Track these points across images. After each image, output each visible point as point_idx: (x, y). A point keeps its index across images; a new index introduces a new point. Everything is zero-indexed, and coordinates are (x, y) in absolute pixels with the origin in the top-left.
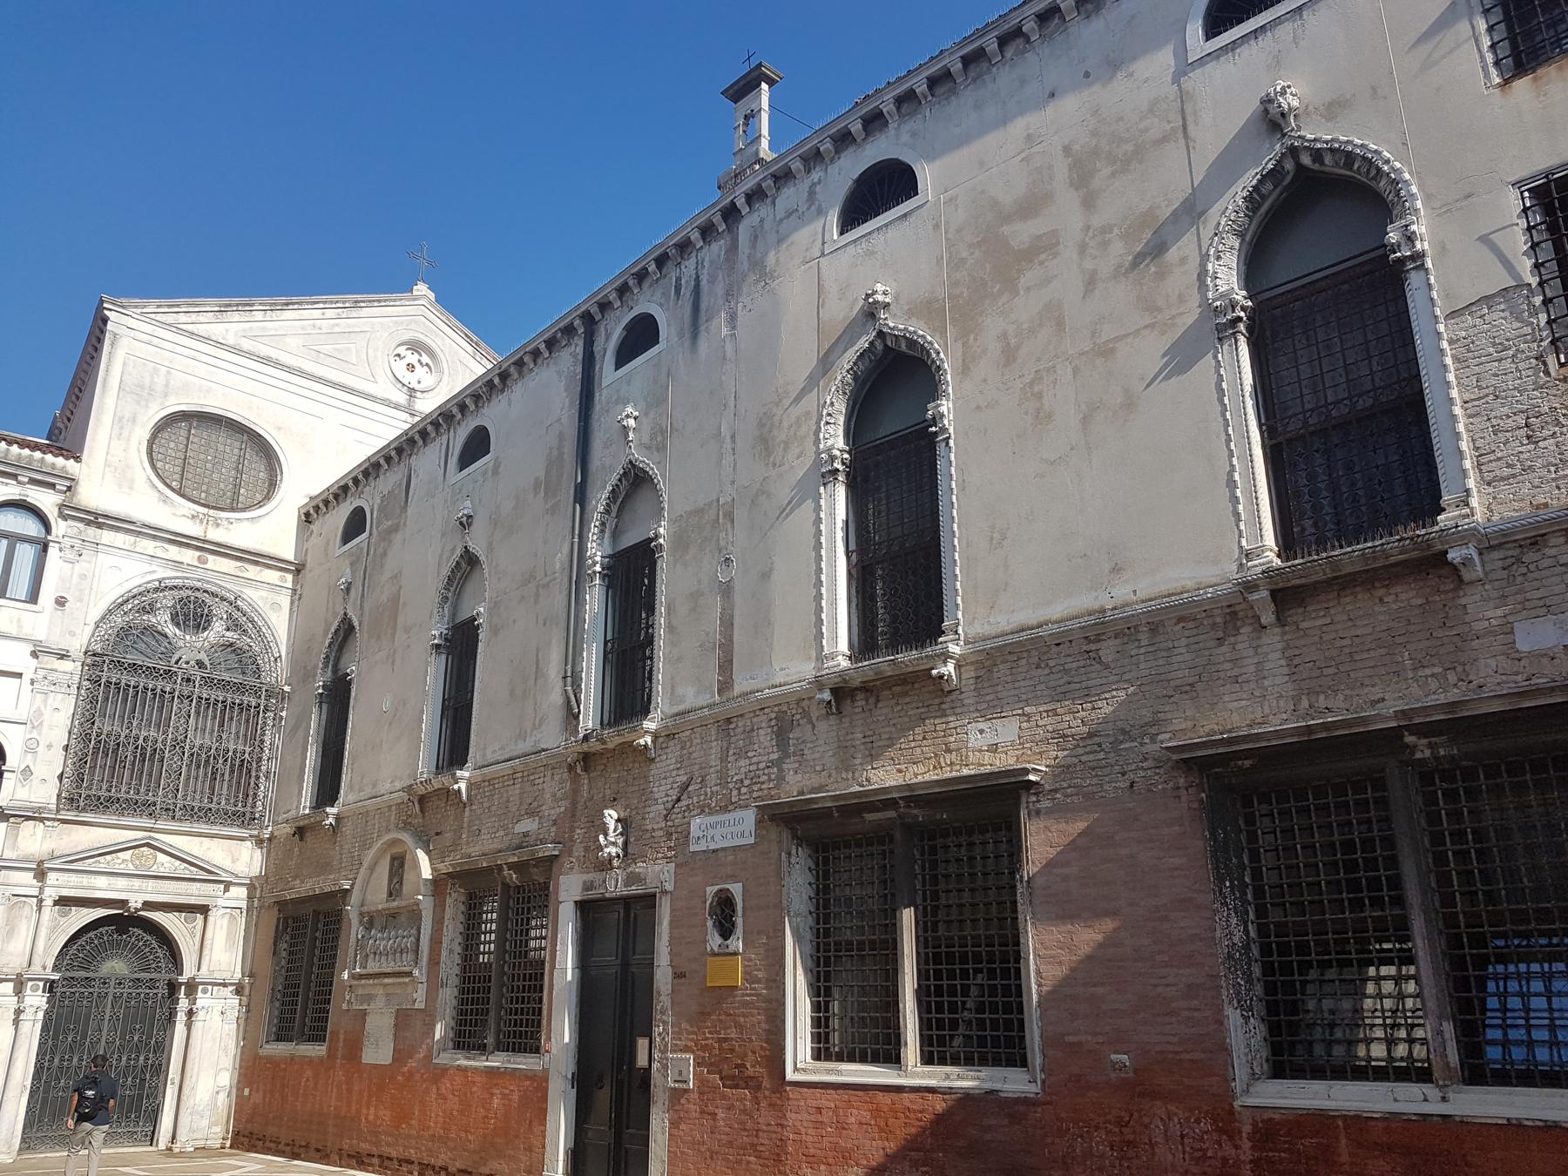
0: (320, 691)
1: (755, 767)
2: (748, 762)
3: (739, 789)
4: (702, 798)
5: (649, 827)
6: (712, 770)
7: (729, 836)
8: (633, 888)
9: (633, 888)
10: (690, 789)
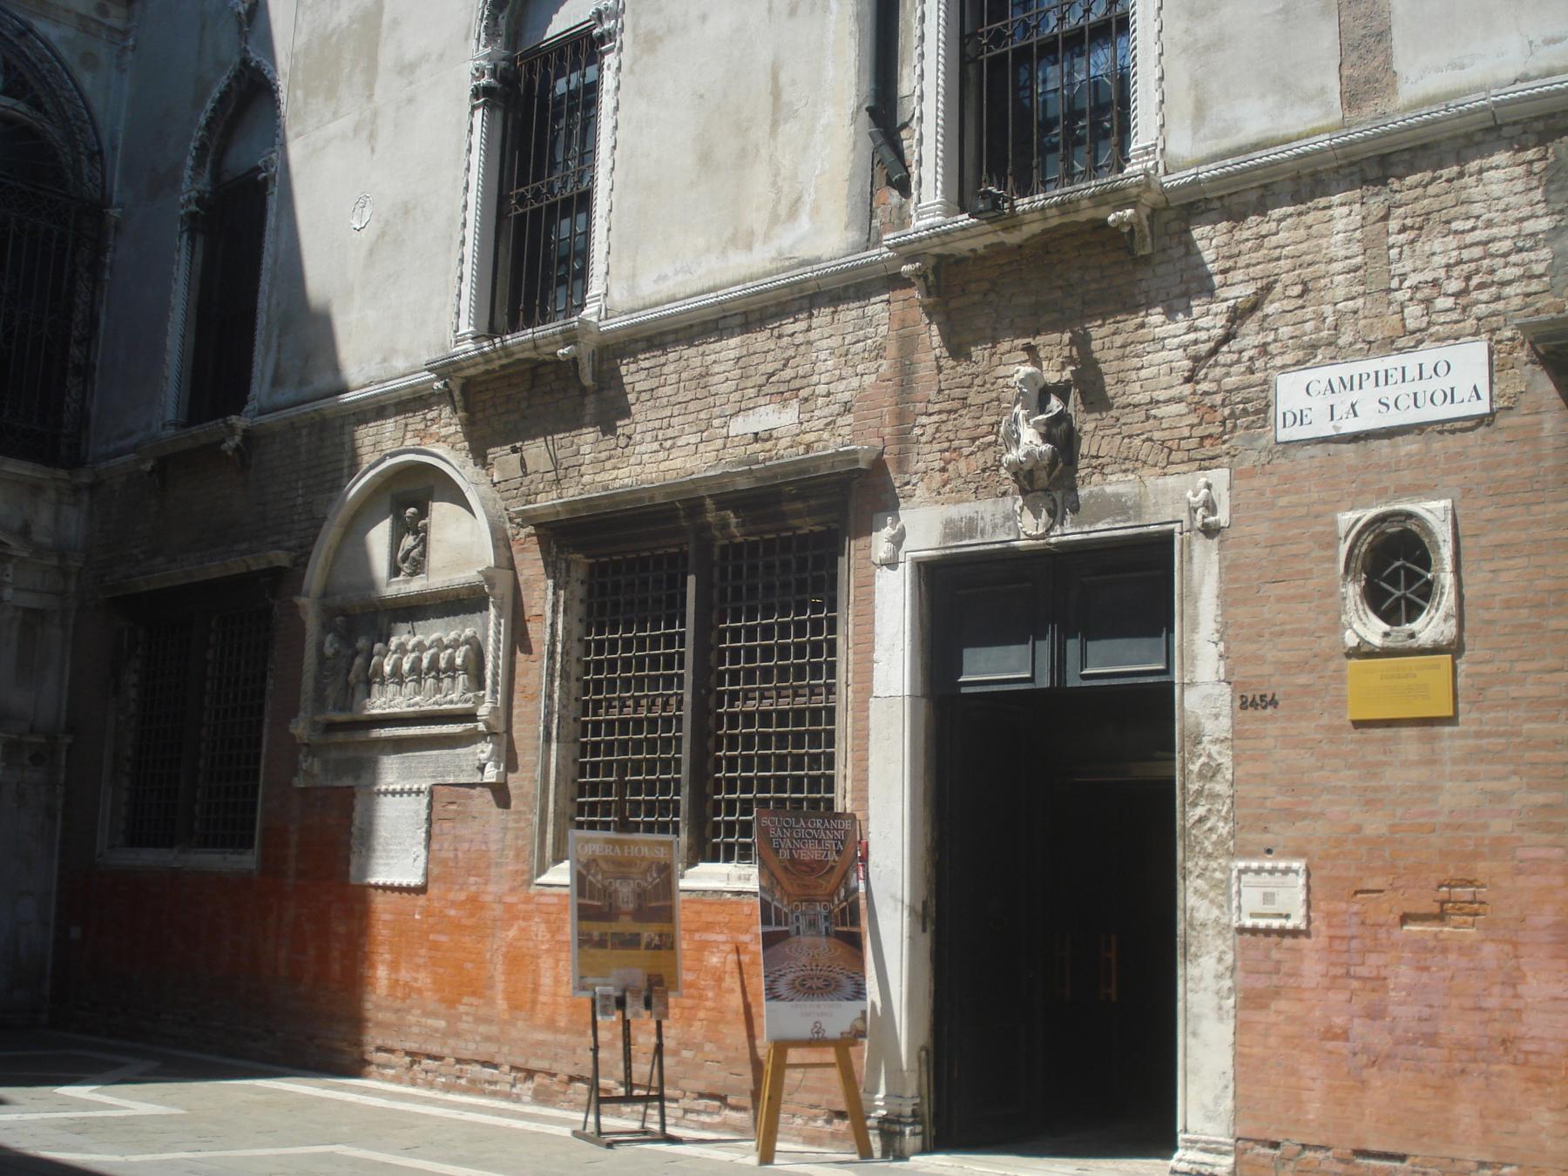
0: (193, 208)
1: (1477, 252)
2: (1452, 242)
3: (1428, 302)
4: (1309, 326)
5: (1143, 398)
6: (1337, 266)
7: (1439, 397)
8: (1100, 526)
9: (1100, 526)
10: (1269, 309)
